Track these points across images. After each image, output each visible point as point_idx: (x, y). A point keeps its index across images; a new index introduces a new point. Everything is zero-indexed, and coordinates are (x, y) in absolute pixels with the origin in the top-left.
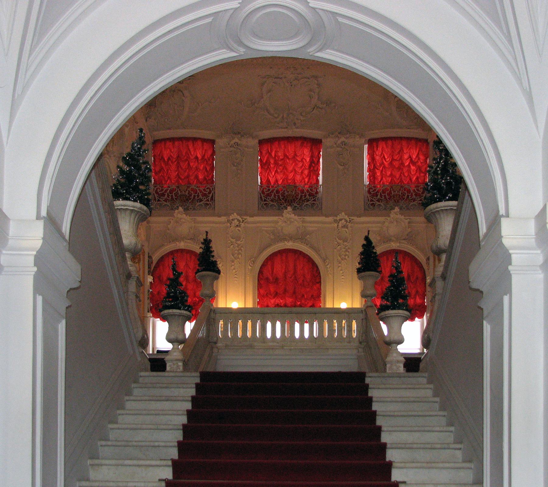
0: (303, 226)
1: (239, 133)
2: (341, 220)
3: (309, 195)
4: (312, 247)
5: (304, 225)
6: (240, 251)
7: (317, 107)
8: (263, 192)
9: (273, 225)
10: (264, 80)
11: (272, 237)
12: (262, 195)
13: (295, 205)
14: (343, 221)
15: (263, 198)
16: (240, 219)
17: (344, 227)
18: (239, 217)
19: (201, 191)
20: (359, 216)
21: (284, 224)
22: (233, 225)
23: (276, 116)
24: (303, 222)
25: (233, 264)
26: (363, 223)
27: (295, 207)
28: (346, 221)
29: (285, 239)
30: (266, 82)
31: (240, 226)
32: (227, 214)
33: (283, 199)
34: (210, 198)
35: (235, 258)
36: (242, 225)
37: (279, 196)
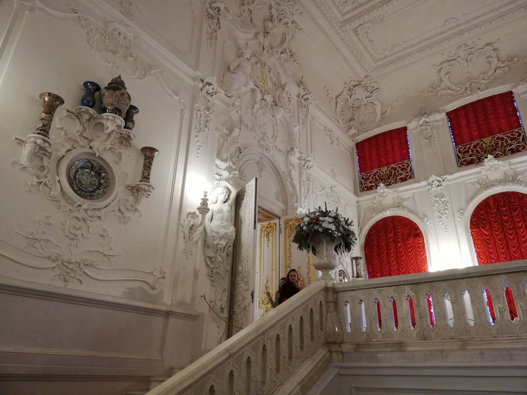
0: (511, 169)
1: (426, 113)
3: (511, 140)
5: (512, 167)
6: (446, 207)
7: (499, 68)
8: (460, 152)
9: (476, 176)
10: (440, 67)
11: (478, 187)
12: (459, 154)
13: (497, 152)
15: (461, 156)
19: (400, 167)
22: (434, 186)
23: (459, 89)
24: (510, 164)
25: (441, 220)
27: (498, 154)
29: (493, 185)
30: (442, 68)
31: (441, 185)
32: (426, 179)
33: (482, 151)
34: (409, 170)
35: (442, 214)
36: (443, 184)
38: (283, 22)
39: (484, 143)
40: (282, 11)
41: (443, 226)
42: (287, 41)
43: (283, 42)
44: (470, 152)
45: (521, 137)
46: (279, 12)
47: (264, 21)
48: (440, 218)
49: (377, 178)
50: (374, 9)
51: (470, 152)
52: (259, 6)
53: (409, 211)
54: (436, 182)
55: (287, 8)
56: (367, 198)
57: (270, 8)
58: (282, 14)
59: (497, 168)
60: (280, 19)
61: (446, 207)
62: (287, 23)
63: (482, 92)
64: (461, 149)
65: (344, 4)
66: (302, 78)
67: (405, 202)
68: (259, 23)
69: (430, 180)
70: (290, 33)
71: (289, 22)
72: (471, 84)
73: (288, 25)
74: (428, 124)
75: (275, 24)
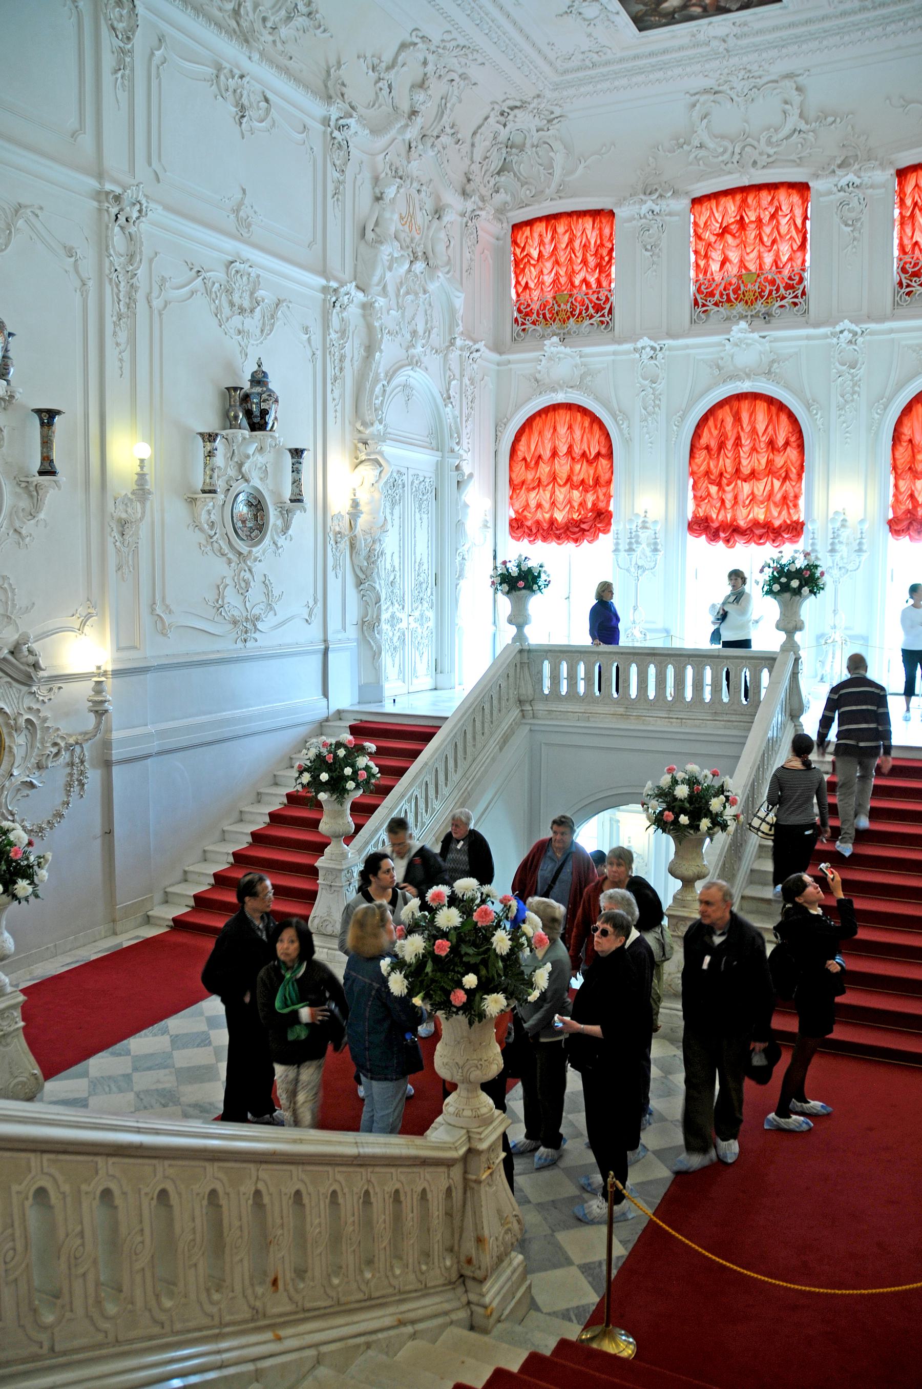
2: (841, 332)
3: (786, 288)
4: (787, 387)
6: (657, 402)
12: (698, 297)
14: (846, 333)
16: (655, 345)
17: (850, 342)
18: (652, 343)
19: (591, 301)
20: (882, 319)
21: (736, 349)
22: (644, 356)
26: (891, 331)
28: (855, 334)
34: (606, 311)
36: (660, 355)
37: (728, 295)
39: (743, 282)
41: (647, 436)
44: (717, 297)
45: (801, 287)
48: (646, 420)
49: (548, 316)
51: (717, 297)
53: (597, 398)
54: (648, 349)
56: (523, 360)
59: (751, 344)
61: (657, 402)
63: (760, 172)
64: (703, 287)
67: (589, 378)
69: (639, 344)
72: (743, 148)
74: (656, 218)
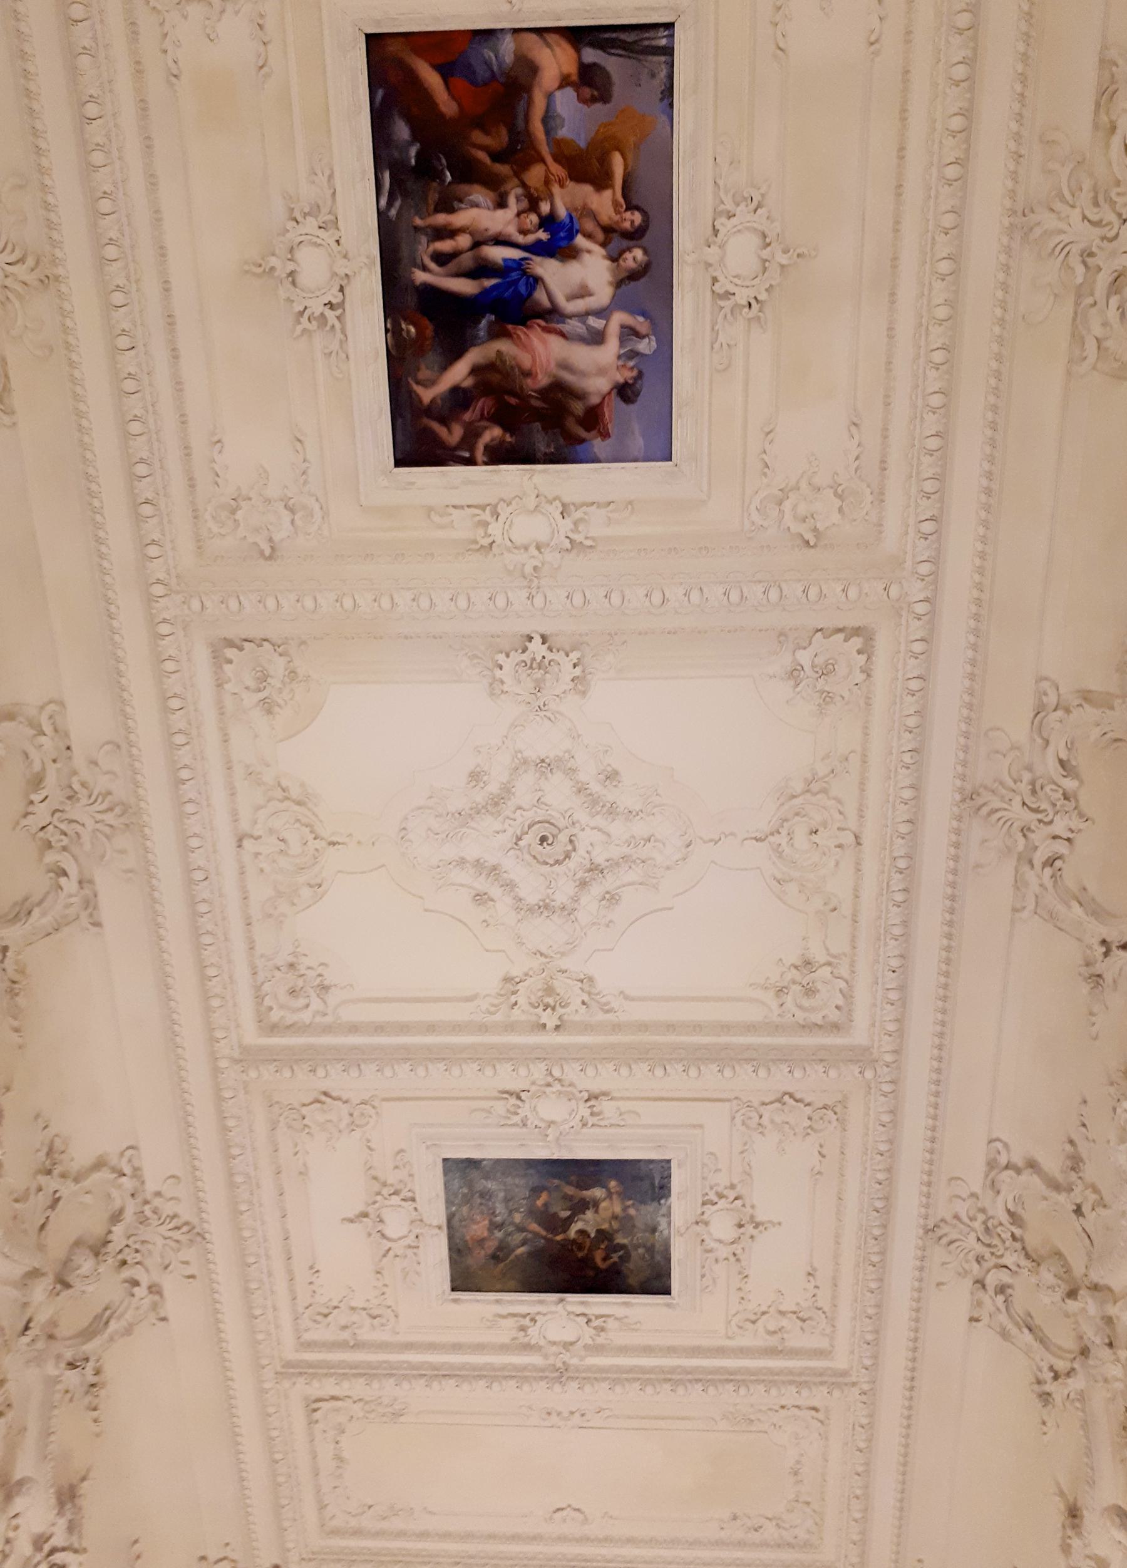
38: (126, 1273)
40: (143, 1242)
42: (106, 1336)
43: (88, 1333)
46: (130, 1242)
47: (77, 1243)
50: (392, 1375)
52: (88, 1199)
55: (160, 1242)
57: (116, 1217)
58: (137, 1251)
60: (124, 1263)
62: (136, 1283)
65: (319, 1318)
66: (83, 1479)
68: (58, 1241)
70: (128, 1316)
71: (145, 1283)
73: (136, 1290)
75: (101, 1269)
